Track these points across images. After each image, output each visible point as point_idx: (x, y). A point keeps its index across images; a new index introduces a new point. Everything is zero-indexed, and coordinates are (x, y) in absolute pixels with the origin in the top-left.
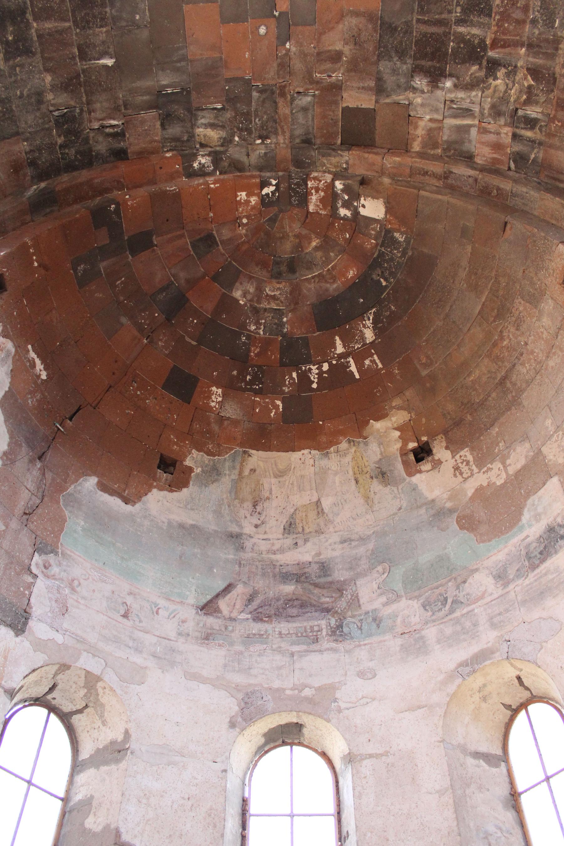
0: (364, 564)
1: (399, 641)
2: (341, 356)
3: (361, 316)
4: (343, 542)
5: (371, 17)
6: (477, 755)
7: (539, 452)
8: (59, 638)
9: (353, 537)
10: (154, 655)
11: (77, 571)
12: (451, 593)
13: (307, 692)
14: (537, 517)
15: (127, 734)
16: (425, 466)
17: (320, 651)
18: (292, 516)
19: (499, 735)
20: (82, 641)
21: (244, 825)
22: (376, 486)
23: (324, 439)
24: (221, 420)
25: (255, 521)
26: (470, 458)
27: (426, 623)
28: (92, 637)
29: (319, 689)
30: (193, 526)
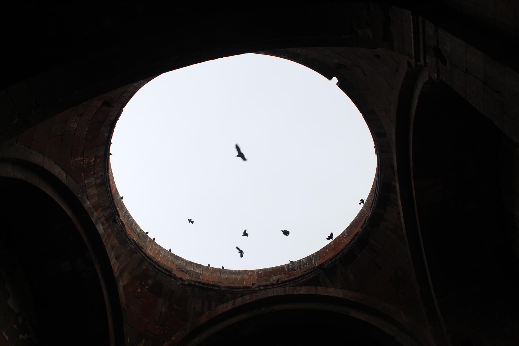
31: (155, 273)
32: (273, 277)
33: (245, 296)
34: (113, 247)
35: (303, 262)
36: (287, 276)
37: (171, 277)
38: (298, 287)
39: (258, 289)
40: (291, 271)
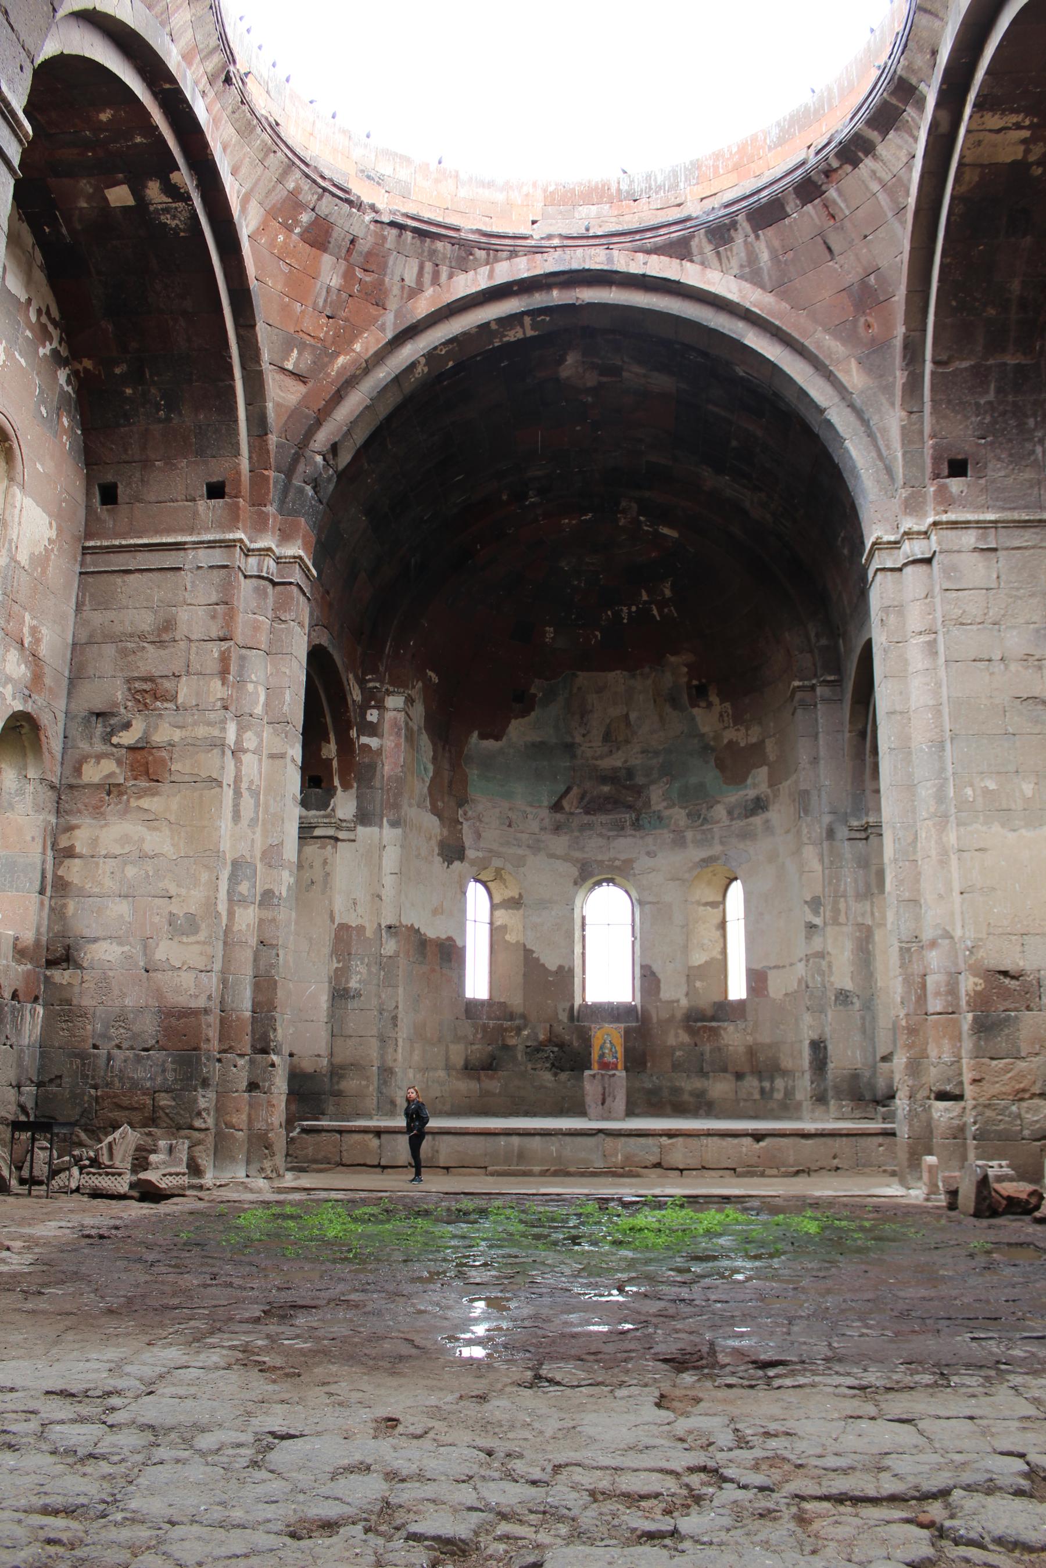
1: (671, 836)
2: (645, 602)
4: (643, 752)
6: (706, 904)
7: (763, 742)
8: (480, 854)
10: (529, 847)
11: (480, 808)
12: (704, 811)
13: (617, 863)
14: (755, 786)
15: (520, 894)
16: (703, 704)
17: (625, 836)
19: (722, 890)
20: (491, 851)
21: (583, 930)
22: (668, 709)
25: (583, 731)
26: (730, 711)
27: (687, 827)
29: (624, 861)
30: (542, 743)
31: (316, 197)
32: (581, 208)
33: (517, 260)
34: (225, 149)
35: (656, 182)
36: (616, 213)
37: (350, 202)
38: (640, 256)
40: (625, 199)
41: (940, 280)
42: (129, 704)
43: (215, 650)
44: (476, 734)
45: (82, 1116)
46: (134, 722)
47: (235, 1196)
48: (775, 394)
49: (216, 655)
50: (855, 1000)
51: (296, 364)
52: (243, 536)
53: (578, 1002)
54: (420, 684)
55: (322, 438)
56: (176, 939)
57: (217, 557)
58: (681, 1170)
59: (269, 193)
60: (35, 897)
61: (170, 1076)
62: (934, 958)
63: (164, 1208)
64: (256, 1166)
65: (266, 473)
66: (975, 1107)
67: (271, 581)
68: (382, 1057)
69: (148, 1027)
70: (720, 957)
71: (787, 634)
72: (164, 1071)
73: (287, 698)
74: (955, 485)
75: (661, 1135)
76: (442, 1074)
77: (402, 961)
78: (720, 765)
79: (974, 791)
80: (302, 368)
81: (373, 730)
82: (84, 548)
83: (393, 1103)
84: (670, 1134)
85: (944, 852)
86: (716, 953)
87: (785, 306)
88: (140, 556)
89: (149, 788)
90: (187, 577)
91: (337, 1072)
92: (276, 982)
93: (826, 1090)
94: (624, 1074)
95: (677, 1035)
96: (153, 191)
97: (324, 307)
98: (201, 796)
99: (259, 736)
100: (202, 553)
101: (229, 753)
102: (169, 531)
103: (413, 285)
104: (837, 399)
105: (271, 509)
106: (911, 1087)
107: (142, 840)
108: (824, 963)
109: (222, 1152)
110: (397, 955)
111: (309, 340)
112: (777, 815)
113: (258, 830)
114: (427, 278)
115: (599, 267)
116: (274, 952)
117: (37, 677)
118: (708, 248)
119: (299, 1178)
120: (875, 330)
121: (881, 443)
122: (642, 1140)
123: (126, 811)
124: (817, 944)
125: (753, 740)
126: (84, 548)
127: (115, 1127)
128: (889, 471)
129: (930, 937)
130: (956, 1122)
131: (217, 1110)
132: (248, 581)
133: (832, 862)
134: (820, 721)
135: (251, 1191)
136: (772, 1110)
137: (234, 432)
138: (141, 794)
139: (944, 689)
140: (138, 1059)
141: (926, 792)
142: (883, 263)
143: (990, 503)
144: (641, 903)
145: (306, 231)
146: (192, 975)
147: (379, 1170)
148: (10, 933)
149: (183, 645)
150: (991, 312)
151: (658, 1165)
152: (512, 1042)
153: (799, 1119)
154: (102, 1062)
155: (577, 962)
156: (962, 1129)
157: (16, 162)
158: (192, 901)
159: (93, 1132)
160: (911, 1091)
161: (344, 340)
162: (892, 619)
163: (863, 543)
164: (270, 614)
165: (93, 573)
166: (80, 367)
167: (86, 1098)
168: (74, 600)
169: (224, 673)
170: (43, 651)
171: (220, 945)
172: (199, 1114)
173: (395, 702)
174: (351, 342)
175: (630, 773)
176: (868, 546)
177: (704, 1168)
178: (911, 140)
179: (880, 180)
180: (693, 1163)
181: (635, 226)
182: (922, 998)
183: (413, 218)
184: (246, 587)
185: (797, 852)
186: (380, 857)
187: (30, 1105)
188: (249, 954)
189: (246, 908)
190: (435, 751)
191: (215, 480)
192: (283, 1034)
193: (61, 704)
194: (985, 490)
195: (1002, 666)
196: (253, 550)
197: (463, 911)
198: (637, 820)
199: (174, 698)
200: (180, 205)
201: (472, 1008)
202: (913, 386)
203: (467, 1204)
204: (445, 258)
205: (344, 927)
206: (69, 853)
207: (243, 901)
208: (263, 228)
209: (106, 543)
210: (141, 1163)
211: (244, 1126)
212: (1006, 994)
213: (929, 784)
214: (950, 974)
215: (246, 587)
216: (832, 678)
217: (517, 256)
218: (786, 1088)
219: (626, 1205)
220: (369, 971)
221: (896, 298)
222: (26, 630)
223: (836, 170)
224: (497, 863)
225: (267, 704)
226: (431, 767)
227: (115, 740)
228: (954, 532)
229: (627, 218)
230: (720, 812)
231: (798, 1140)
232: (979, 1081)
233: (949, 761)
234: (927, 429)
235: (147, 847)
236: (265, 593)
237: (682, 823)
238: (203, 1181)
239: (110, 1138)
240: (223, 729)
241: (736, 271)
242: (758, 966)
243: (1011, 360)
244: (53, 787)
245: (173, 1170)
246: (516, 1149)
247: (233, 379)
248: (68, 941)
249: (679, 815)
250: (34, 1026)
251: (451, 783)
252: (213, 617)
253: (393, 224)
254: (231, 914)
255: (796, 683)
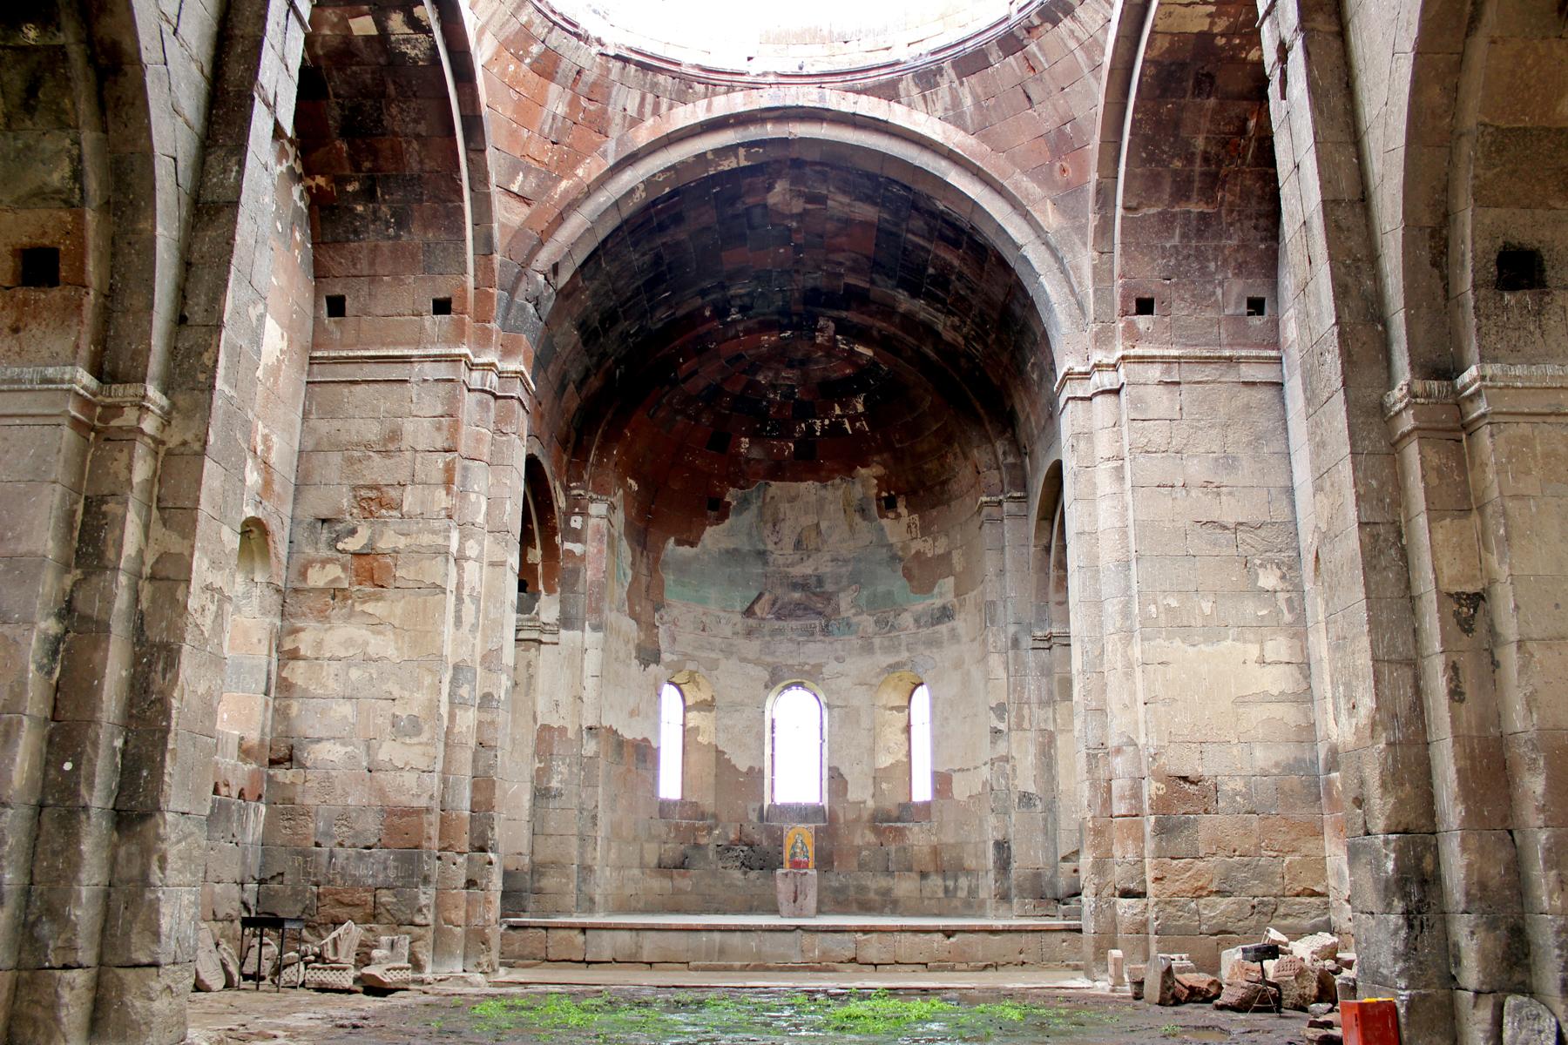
0: (845, 582)
2: (838, 416)
3: (855, 394)
5: (868, 258)
6: (892, 708)
7: (950, 553)
8: (675, 658)
9: (841, 558)
10: (721, 651)
11: (676, 612)
12: (891, 619)
13: (807, 668)
14: (941, 595)
16: (891, 515)
18: (800, 534)
20: (685, 654)
22: (857, 518)
23: (823, 474)
24: (748, 461)
28: (689, 650)
29: (813, 666)
30: (736, 550)
33: (735, 94)
38: (851, 96)
39: (761, 79)
41: (1132, 134)
42: (355, 511)
43: (440, 460)
44: (672, 540)
45: (303, 912)
46: (359, 529)
47: (457, 990)
48: (972, 228)
49: (441, 466)
50: (1038, 802)
51: (521, 187)
52: (468, 351)
53: (767, 802)
54: (621, 492)
55: (544, 258)
56: (399, 740)
57: (443, 370)
58: (876, 965)
59: (503, 26)
60: (261, 698)
61: (392, 874)
62: (1119, 764)
63: (393, 1000)
64: (472, 961)
65: (491, 290)
66: (1157, 904)
67: (493, 395)
68: (582, 855)
69: (371, 826)
70: (905, 760)
71: (975, 451)
72: (385, 869)
73: (508, 507)
74: (1143, 321)
75: (856, 931)
76: (636, 872)
77: (602, 762)
78: (908, 574)
79: (1157, 608)
80: (527, 191)
81: (577, 536)
82: (311, 358)
83: (592, 900)
84: (865, 931)
85: (1129, 666)
86: (901, 756)
87: (986, 148)
88: (366, 367)
89: (374, 594)
90: (413, 390)
91: (537, 870)
92: (494, 782)
93: (1009, 888)
94: (815, 872)
95: (863, 836)
96: (396, 22)
97: (550, 133)
98: (425, 601)
99: (481, 544)
100: (428, 366)
101: (452, 561)
102: (396, 344)
103: (635, 115)
104: (1032, 237)
105: (494, 326)
106: (1097, 886)
107: (367, 643)
108: (1008, 767)
109: (440, 948)
110: (597, 755)
111: (534, 165)
112: (962, 624)
113: (479, 635)
114: (648, 108)
115: (811, 105)
116: (493, 753)
117: (267, 484)
118: (915, 91)
119: (507, 974)
120: (1070, 174)
121: (1073, 280)
122: (838, 936)
123: (351, 614)
124: (1002, 747)
125: (940, 551)
126: (311, 358)
127: (337, 923)
128: (1081, 306)
129: (1115, 744)
130: (1139, 918)
131: (437, 906)
132: (471, 394)
133: (1016, 671)
134: (1007, 535)
135: (471, 984)
136: (956, 908)
137: (462, 251)
138: (365, 599)
139: (1131, 513)
140: (360, 857)
141: (1112, 608)
142: (1079, 114)
143: (1174, 339)
144: (829, 706)
145: (536, 61)
146: (415, 775)
147: (584, 965)
148: (237, 733)
149: (408, 454)
150: (1177, 164)
151: (853, 960)
152: (703, 841)
153: (982, 916)
154: (324, 859)
155: (767, 763)
156: (1145, 924)
157: (306, 18)
158: (415, 703)
159: (314, 928)
160: (1097, 889)
161: (567, 165)
162: (1082, 445)
163: (1054, 370)
164: (492, 427)
165: (320, 382)
166: (313, 184)
167: (308, 895)
168: (301, 409)
169: (448, 483)
170: (273, 458)
171: (441, 746)
172: (420, 910)
173: (597, 509)
174: (574, 167)
175: (820, 581)
176: (1059, 378)
177: (897, 963)
178: (1107, 6)
179: (1078, 39)
180: (887, 958)
181: (845, 67)
182: (1107, 802)
183: (637, 52)
184: (470, 400)
185: (983, 659)
186: (582, 659)
187: (252, 902)
188: (469, 755)
189: (466, 710)
190: (634, 557)
191: (441, 296)
192: (499, 833)
193: (287, 510)
194: (1169, 327)
195: (1184, 492)
196: (477, 365)
197: (658, 713)
198: (827, 626)
199: (399, 506)
200: (422, 36)
201: (665, 808)
202: (1104, 229)
203: (683, 996)
204: (666, 90)
205: (546, 728)
206: (294, 655)
207: (464, 704)
208: (496, 57)
209: (333, 354)
210: (364, 959)
211: (463, 924)
212: (1187, 798)
213: (1115, 601)
214: (1133, 779)
215: (470, 400)
216: (1015, 495)
217: (734, 91)
218: (970, 887)
219: (835, 997)
220: (571, 772)
221: (1090, 147)
222: (259, 439)
223: (1037, 27)
224: (691, 666)
225: (488, 514)
226: (629, 573)
227: (340, 546)
228: (1141, 365)
229: (837, 59)
230: (907, 619)
231: (986, 936)
232: (1161, 879)
233: (1134, 580)
234: (1117, 270)
235: (371, 651)
236: (488, 405)
237: (870, 630)
238: (423, 976)
239: (334, 934)
240: (448, 538)
241: (940, 113)
242: (942, 769)
243: (1195, 208)
244: (278, 591)
245: (396, 965)
246: (717, 944)
247: (462, 201)
248: (291, 741)
249: (867, 622)
250: (257, 823)
251: (648, 588)
252: (439, 429)
253: (617, 57)
254: (452, 717)
255: (984, 499)
